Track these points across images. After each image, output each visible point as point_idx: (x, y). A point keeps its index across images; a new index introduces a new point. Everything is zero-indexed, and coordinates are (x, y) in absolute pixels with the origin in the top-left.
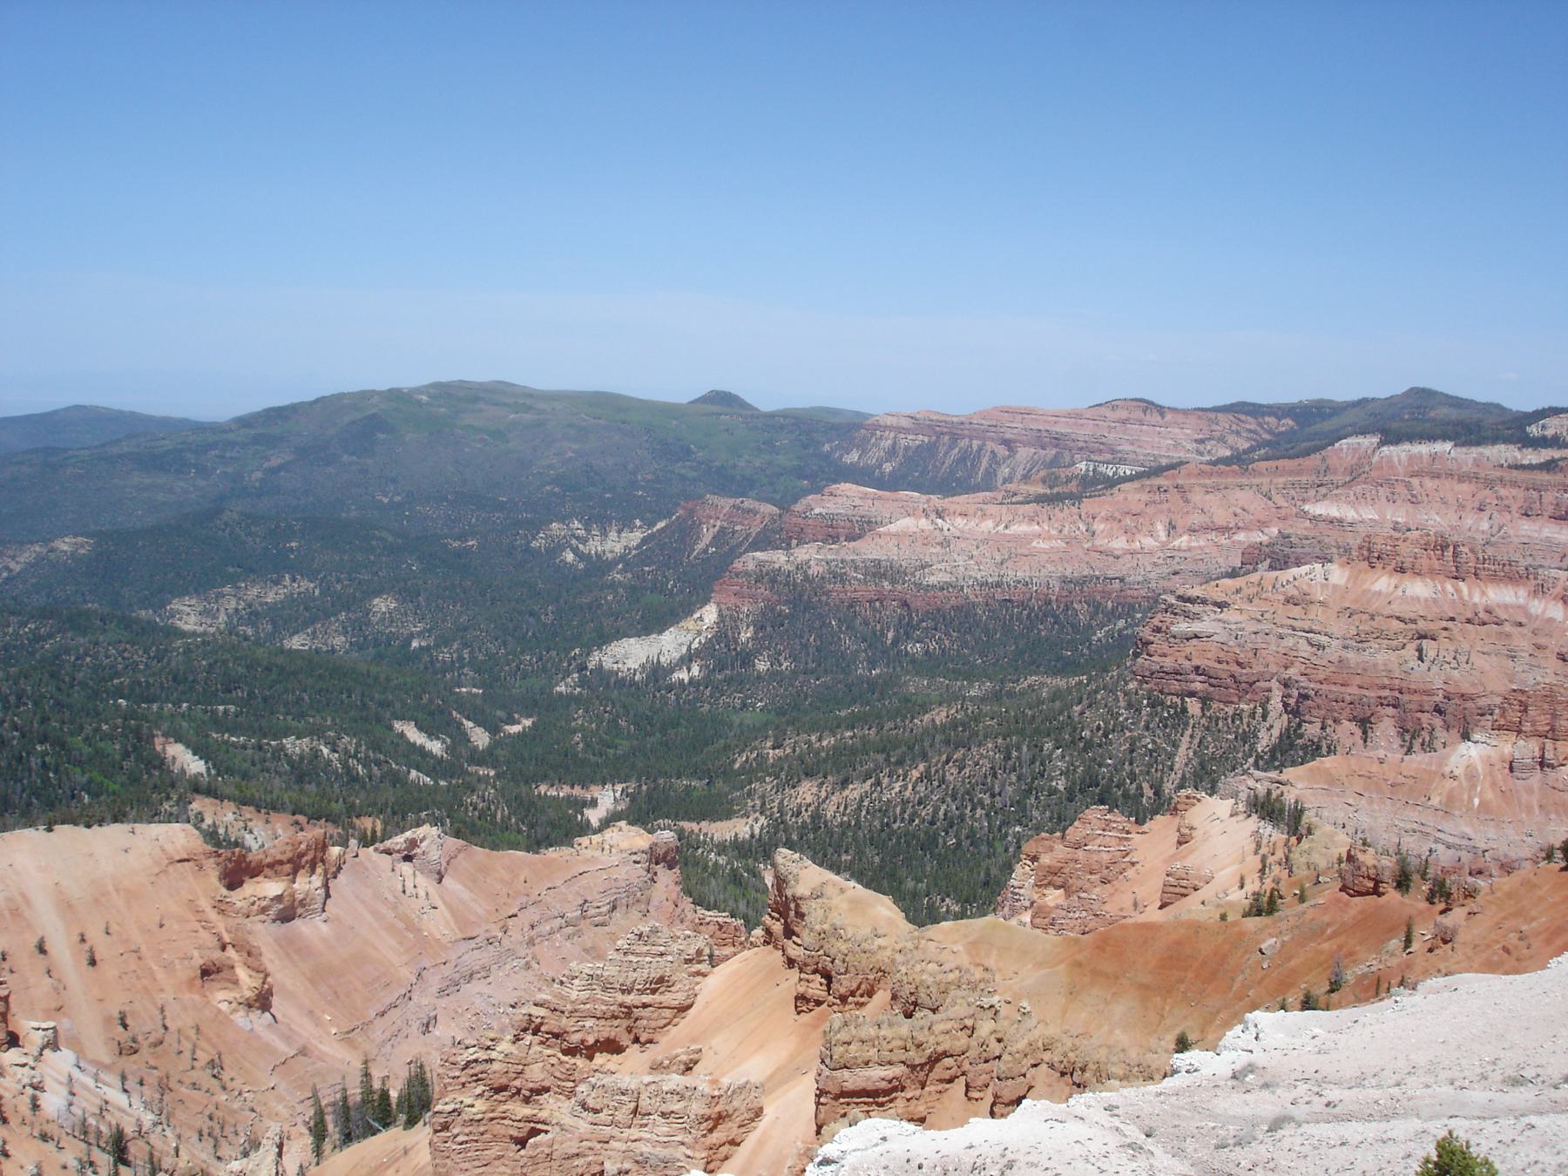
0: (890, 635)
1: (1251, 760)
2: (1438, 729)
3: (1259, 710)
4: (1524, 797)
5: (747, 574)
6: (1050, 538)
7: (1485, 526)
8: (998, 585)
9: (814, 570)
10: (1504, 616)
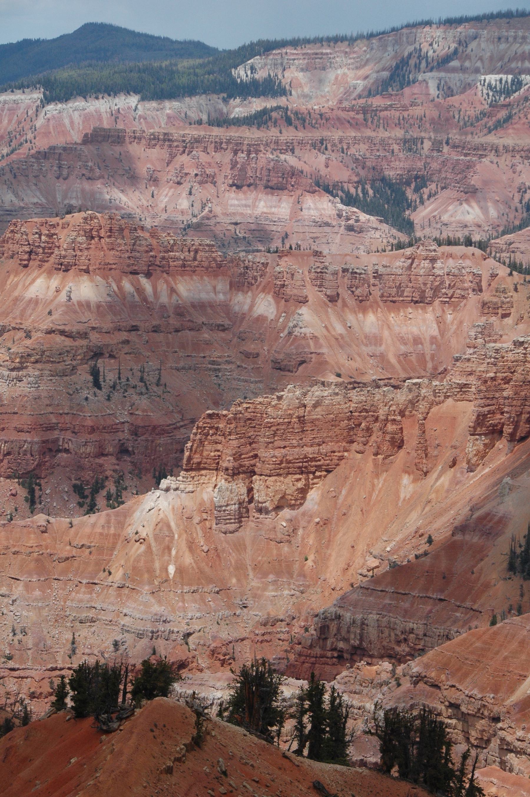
7: (184, 204)
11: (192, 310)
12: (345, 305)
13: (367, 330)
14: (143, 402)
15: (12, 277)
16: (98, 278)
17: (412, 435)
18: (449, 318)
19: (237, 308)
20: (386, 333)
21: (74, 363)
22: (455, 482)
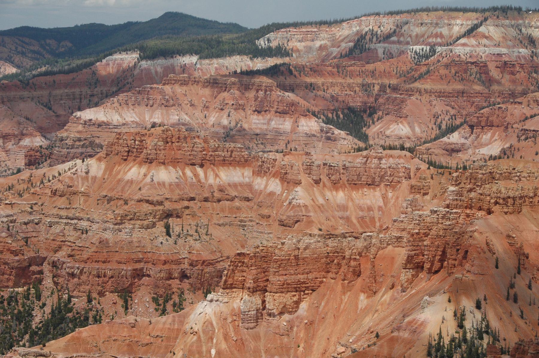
1: (27, 337)
2: (187, 292)
3: (33, 291)
4: (252, 345)
10: (234, 193)
11: (228, 188)
12: (324, 185)
13: (338, 202)
14: (197, 245)
15: (117, 166)
16: (171, 168)
17: (366, 268)
18: (390, 195)
19: (256, 187)
20: (350, 204)
21: (154, 220)
22: (393, 299)
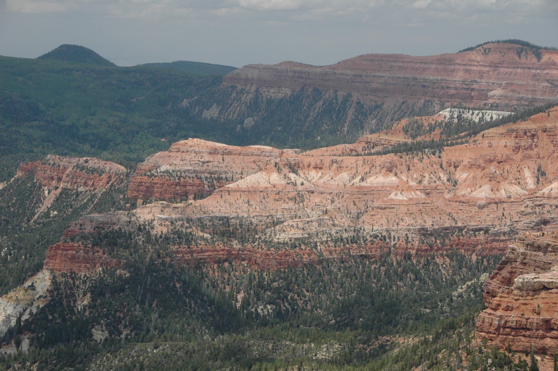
0: (240, 297)
5: (84, 237)
6: (410, 188)
8: (354, 240)
9: (159, 230)
